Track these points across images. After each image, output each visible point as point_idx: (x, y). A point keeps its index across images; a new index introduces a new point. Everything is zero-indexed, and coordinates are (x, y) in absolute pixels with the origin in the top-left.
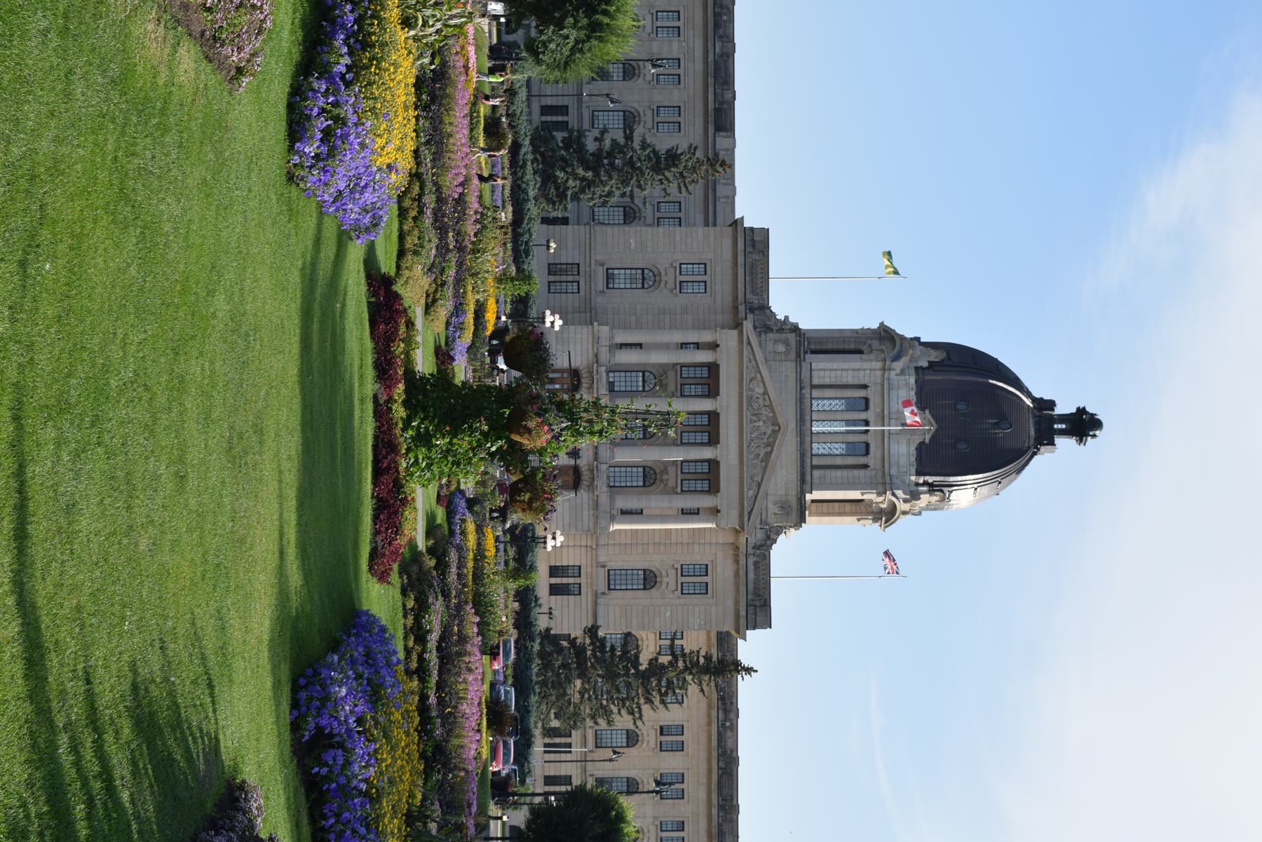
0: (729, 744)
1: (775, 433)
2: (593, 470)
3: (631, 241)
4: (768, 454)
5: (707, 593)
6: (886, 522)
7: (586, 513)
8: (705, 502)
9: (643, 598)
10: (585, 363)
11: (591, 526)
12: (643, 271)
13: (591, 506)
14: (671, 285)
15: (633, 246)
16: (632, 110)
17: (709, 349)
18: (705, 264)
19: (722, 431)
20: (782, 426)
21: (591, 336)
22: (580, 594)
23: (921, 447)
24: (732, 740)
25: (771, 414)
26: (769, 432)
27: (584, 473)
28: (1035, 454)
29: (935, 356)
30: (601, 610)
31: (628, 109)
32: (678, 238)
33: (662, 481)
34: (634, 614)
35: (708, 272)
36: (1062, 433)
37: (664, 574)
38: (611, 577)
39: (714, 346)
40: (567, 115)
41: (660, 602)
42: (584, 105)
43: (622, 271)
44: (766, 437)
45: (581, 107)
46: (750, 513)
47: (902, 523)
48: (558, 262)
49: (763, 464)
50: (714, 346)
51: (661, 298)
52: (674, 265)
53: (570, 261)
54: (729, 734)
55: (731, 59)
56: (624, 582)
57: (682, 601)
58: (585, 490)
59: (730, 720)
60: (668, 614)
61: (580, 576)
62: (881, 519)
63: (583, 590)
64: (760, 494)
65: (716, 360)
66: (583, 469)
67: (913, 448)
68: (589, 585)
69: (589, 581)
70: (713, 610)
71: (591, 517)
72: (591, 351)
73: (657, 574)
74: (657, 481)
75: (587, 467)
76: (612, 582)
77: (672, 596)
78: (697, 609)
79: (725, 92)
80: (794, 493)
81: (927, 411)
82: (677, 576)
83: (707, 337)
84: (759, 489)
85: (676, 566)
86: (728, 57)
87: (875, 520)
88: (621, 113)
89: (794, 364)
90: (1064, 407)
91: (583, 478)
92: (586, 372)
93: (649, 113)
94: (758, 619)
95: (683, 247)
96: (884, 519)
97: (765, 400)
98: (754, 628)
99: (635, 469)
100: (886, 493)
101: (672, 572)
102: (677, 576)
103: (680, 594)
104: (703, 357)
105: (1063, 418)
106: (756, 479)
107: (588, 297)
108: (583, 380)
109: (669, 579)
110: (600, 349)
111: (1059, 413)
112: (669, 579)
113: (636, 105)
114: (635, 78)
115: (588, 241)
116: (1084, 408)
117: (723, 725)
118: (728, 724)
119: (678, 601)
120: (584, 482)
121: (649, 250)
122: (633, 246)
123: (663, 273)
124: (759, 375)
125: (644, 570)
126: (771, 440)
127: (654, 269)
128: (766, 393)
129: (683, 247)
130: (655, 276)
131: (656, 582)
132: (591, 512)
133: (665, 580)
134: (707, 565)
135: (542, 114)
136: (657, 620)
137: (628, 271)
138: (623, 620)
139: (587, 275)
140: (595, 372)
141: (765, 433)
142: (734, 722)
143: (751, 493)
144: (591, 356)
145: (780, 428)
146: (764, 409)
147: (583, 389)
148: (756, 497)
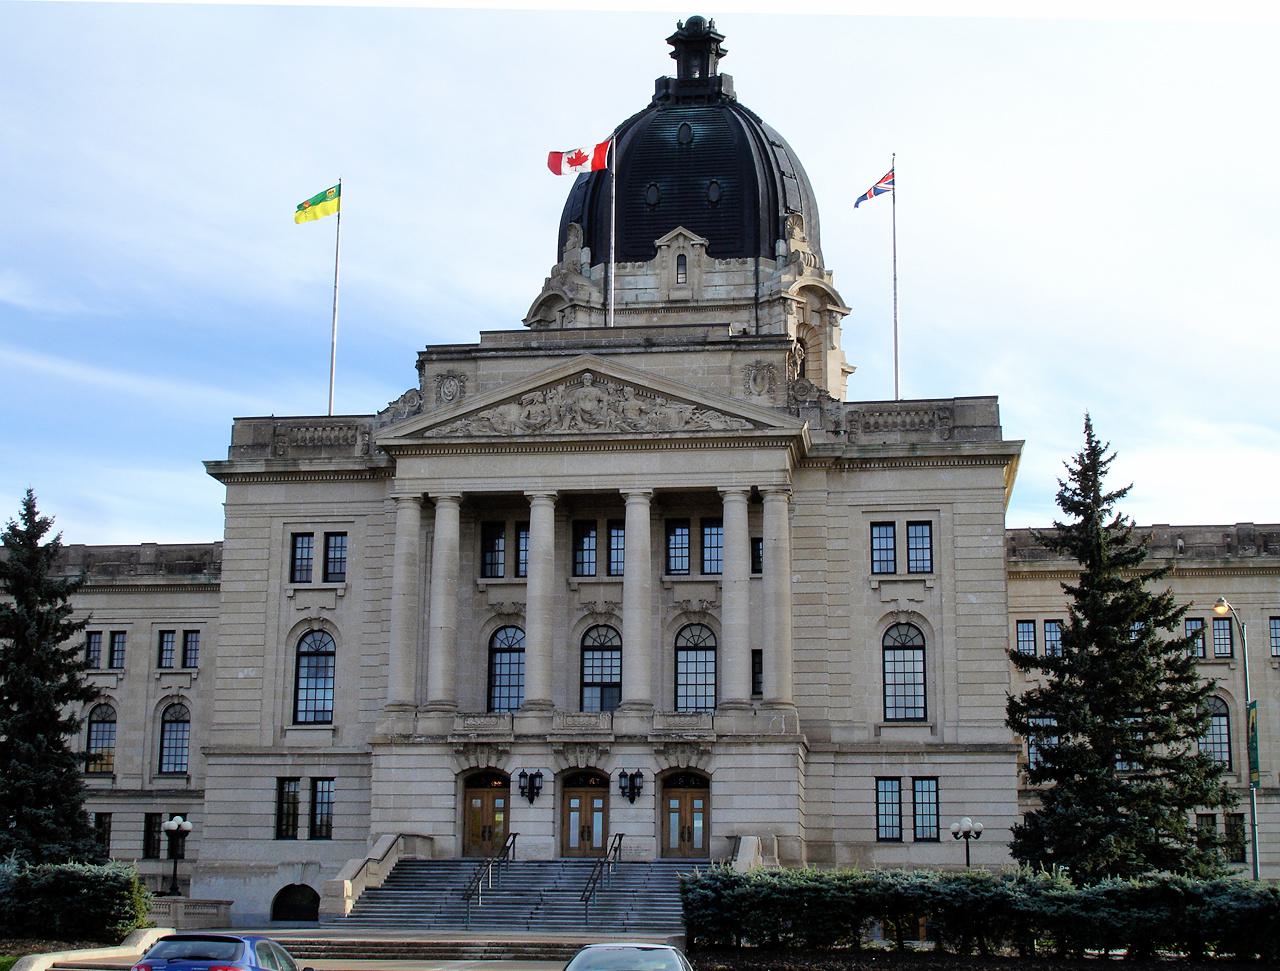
0: (1212, 539)
1: (598, 379)
2: (666, 744)
3: (241, 675)
4: (641, 391)
5: (929, 523)
6: (836, 304)
7: (758, 761)
8: (735, 512)
9: (944, 647)
10: (448, 761)
11: (784, 749)
12: (308, 654)
13: (742, 749)
14: (328, 599)
15: (252, 673)
16: (162, 708)
17: (434, 518)
18: (295, 536)
19: (594, 484)
20: (583, 367)
21: (395, 750)
22: (935, 778)
23: (711, 252)
24: (1209, 535)
25: (561, 388)
26: (595, 392)
27: (674, 764)
28: (733, 103)
29: (576, 236)
30: (967, 737)
31: (159, 715)
32: (242, 587)
33: (703, 613)
34: (974, 666)
35: (308, 529)
36: (704, 70)
37: (891, 607)
38: (901, 714)
39: (428, 505)
40: (160, 815)
41: (948, 615)
42: (148, 787)
43: (302, 695)
44: (605, 397)
45: (151, 791)
46: (757, 424)
47: (839, 285)
48: (272, 821)
49: (659, 401)
50: (428, 505)
51: (350, 619)
52: (291, 593)
53: (272, 795)
54: (1197, 540)
55: (93, 551)
56: (910, 690)
57: (945, 572)
58: (708, 763)
59: (1174, 538)
60: (972, 598)
61: (898, 779)
62: (831, 311)
63: (927, 771)
64: (719, 406)
65: (453, 498)
66: (666, 767)
67: (719, 264)
68: (916, 759)
69: (906, 759)
70: (963, 508)
71: (766, 749)
72: (424, 750)
73: (891, 621)
74: (705, 622)
75: (661, 759)
76: (910, 714)
77: (936, 592)
78: (960, 542)
79: (142, 561)
80: (728, 356)
81: (658, 242)
82: (895, 582)
83: (410, 515)
84: (710, 408)
85: (875, 585)
86: (90, 555)
87: (833, 324)
88: (167, 726)
89: (482, 363)
90: (671, 69)
91: (683, 766)
92: (467, 759)
93: (167, 681)
94: (979, 423)
95: (258, 577)
96: (830, 307)
97: (532, 402)
98: (997, 428)
99: (682, 668)
100: (785, 299)
101: (888, 592)
102: (895, 582)
103: (932, 576)
104: (448, 521)
105: (684, 68)
106: (687, 414)
107: (343, 760)
108: (483, 766)
109: (903, 596)
110: (420, 731)
111: (676, 74)
112: (903, 596)
113: (154, 702)
114: (112, 703)
115: (235, 760)
116: (671, 41)
117: (1182, 550)
118: (1180, 542)
119: (947, 580)
120: (692, 764)
121: (259, 640)
122: (252, 673)
123: (304, 615)
124: (482, 414)
125: (885, 648)
126: (611, 386)
127: (304, 629)
128: (516, 399)
129: (258, 577)
130: (312, 631)
131: (909, 624)
132: (755, 749)
133: (905, 606)
134: (873, 524)
135: (156, 857)
136: (984, 621)
137: (303, 683)
138: (987, 689)
139: (301, 761)
140: (463, 740)
141: (599, 401)
142: (1178, 531)
143: (716, 424)
144: (435, 750)
145: (588, 370)
146: (549, 402)
147: (500, 767)
148: (725, 413)
